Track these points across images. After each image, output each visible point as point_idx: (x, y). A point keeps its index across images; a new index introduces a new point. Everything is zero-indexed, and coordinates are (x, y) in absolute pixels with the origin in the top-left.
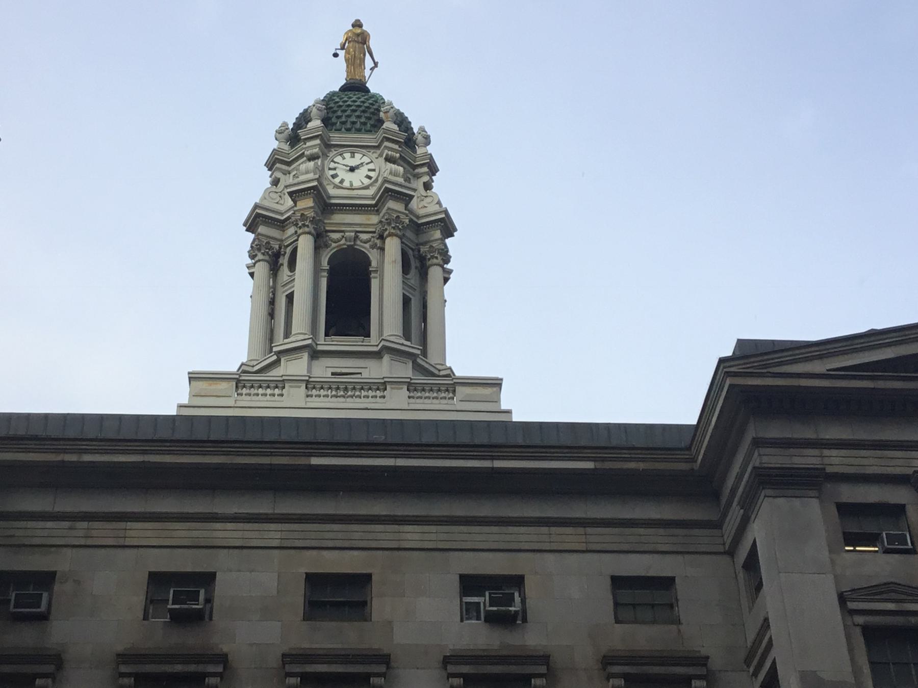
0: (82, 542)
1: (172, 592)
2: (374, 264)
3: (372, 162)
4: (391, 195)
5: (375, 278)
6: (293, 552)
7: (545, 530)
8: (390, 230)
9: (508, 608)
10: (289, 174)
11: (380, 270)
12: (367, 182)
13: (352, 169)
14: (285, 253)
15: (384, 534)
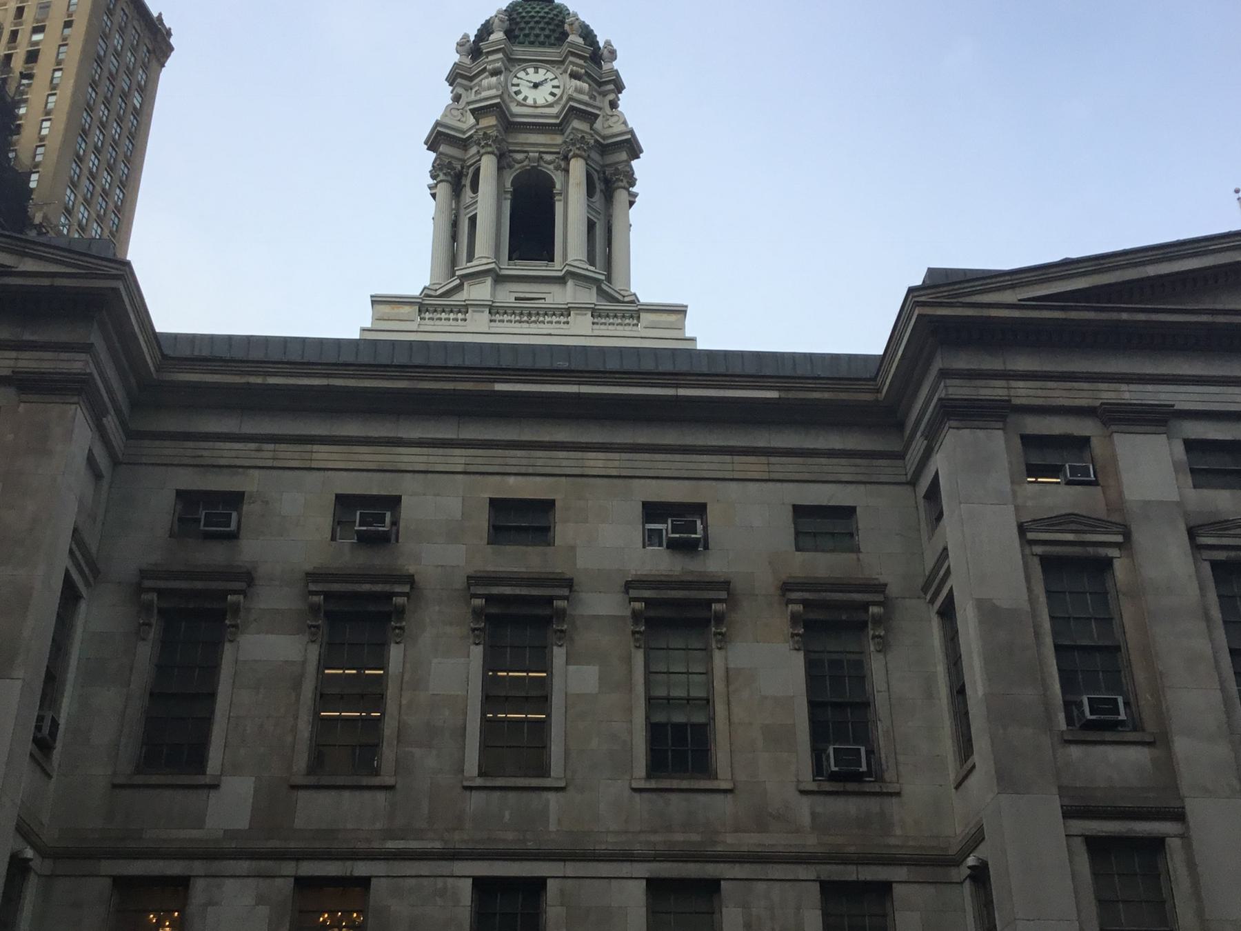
0: (270, 463)
2: (558, 186)
3: (556, 78)
4: (576, 114)
5: (560, 200)
7: (728, 458)
8: (574, 150)
9: (689, 535)
10: (471, 89)
11: (565, 192)
12: (551, 99)
13: (536, 86)
14: (468, 173)
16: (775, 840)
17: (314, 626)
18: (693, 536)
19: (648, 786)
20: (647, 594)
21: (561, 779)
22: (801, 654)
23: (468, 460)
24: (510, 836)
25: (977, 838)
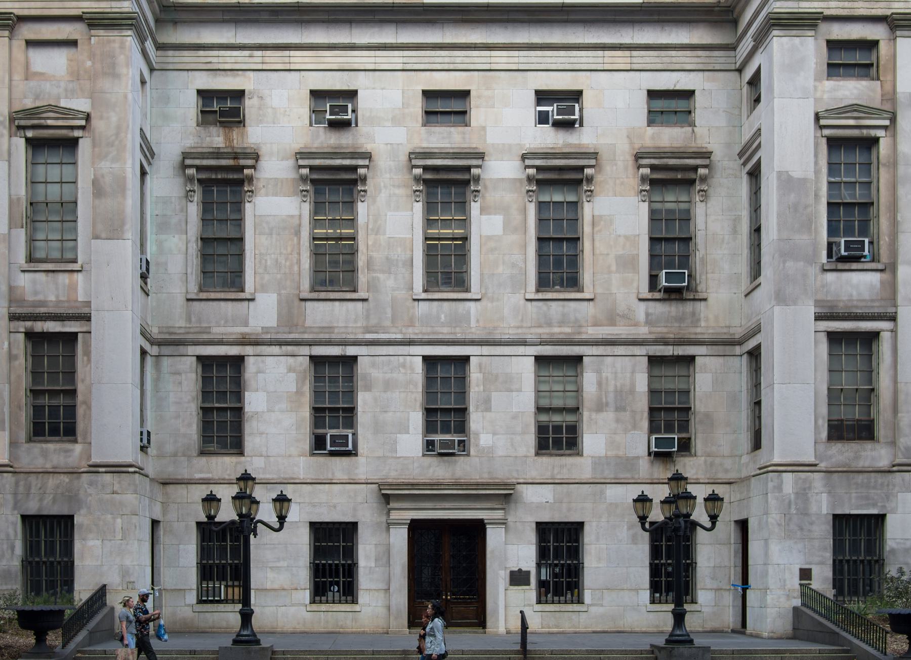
0: (260, 67)
1: (328, 105)
6: (413, 73)
15: (479, 58)
16: (621, 331)
17: (305, 191)
18: (572, 117)
19: (537, 297)
20: (538, 162)
21: (478, 293)
22: (646, 204)
23: (405, 60)
24: (445, 330)
25: (757, 330)
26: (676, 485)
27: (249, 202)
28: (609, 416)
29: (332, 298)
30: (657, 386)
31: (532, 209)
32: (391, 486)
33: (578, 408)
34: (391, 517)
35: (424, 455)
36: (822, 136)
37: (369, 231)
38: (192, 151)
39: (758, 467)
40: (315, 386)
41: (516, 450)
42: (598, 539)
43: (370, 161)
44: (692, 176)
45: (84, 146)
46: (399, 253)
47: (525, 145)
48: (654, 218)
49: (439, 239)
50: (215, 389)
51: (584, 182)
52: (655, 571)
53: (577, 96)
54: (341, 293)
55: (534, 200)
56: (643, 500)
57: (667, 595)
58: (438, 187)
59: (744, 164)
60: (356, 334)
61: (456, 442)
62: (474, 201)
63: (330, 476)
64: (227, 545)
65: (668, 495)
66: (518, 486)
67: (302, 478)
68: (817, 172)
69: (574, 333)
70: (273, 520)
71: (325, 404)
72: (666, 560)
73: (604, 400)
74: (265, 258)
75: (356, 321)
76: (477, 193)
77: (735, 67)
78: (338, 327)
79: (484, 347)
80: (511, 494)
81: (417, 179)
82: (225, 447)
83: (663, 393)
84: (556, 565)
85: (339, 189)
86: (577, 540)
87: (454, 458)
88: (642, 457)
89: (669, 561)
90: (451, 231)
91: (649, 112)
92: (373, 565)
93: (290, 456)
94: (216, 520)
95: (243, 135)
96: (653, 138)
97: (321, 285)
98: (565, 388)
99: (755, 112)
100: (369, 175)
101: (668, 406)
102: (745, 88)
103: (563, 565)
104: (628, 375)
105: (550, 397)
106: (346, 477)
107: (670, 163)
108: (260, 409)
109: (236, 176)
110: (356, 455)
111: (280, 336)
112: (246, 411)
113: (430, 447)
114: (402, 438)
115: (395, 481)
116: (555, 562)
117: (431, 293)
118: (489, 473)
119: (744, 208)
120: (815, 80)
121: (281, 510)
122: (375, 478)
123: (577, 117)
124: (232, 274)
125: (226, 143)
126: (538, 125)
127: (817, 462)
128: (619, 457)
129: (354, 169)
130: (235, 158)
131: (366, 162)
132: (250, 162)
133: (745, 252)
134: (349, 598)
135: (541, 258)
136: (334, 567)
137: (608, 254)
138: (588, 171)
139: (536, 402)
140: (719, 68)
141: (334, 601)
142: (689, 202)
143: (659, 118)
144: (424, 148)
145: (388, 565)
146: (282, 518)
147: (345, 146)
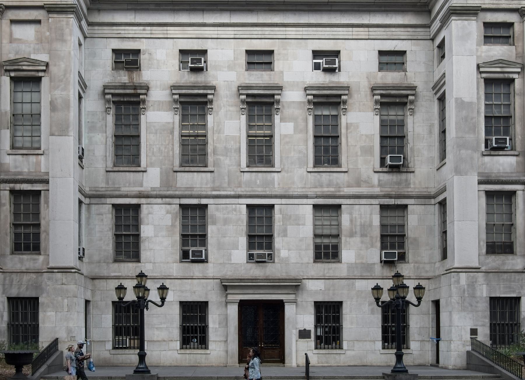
0: (149, 36)
16: (364, 190)
17: (176, 108)
19: (314, 170)
20: (314, 92)
21: (279, 168)
22: (378, 116)
23: (235, 33)
24: (260, 189)
25: (444, 190)
26: (397, 280)
27: (143, 114)
28: (357, 239)
29: (192, 170)
30: (385, 222)
31: (311, 119)
32: (228, 280)
33: (339, 235)
34: (228, 299)
35: (247, 262)
36: (481, 78)
37: (215, 132)
38: (109, 85)
39: (445, 269)
40: (182, 222)
41: (302, 259)
42: (351, 311)
43: (215, 91)
44: (405, 100)
45: (45, 81)
46: (232, 145)
47: (306, 82)
48: (383, 124)
49: (256, 136)
50: (123, 224)
51: (341, 104)
52: (385, 330)
53: (337, 54)
54: (198, 168)
55: (312, 114)
56: (377, 289)
57: (392, 344)
58: (255, 106)
59: (436, 94)
60: (207, 191)
61: (267, 255)
62: (277, 114)
63: (192, 275)
64: (130, 315)
65: (392, 286)
66: (304, 281)
67: (175, 275)
68: (478, 98)
69: (336, 191)
70: (158, 300)
71: (189, 232)
72: (392, 324)
73: (354, 230)
74: (153, 147)
75: (207, 184)
76: (278, 110)
77: (430, 37)
78: (196, 187)
79: (283, 199)
80: (299, 285)
81: (243, 102)
82: (129, 257)
83: (389, 226)
84: (326, 327)
85: (197, 107)
86: (339, 312)
87: (265, 264)
88: (377, 264)
89: (393, 324)
90: (263, 132)
91: (380, 63)
92: (217, 326)
93: (168, 263)
94: (124, 300)
95: (139, 76)
96: (382, 78)
97: (186, 163)
98: (331, 223)
99: (442, 64)
100: (214, 99)
101: (392, 234)
102: (436, 50)
103: (330, 327)
104: (368, 216)
105: (322, 229)
106: (201, 275)
107: (392, 93)
108: (150, 235)
109: (135, 100)
110: (207, 262)
111: (161, 193)
112: (141, 236)
113: (251, 258)
114: (235, 252)
115: (230, 277)
116: (325, 325)
117: (252, 168)
118: (286, 273)
119: (436, 119)
120: (477, 45)
121: (163, 294)
122: (218, 275)
123: (337, 66)
124: (133, 156)
125: (129, 80)
126: (314, 71)
127: (480, 267)
128: (364, 264)
129: (205, 95)
130: (134, 89)
131: (213, 92)
132: (143, 91)
133: (437, 144)
134: (203, 346)
135: (316, 147)
136: (194, 328)
137: (356, 146)
138: (344, 97)
139: (314, 231)
140: (420, 38)
141: (194, 347)
142: (403, 115)
143: (385, 67)
144: (247, 83)
145: (226, 327)
146: (163, 299)
147: (200, 82)
